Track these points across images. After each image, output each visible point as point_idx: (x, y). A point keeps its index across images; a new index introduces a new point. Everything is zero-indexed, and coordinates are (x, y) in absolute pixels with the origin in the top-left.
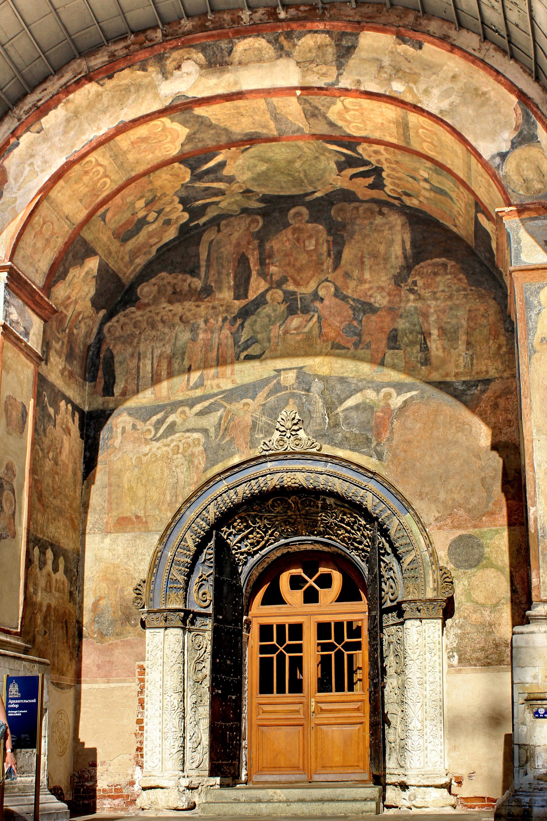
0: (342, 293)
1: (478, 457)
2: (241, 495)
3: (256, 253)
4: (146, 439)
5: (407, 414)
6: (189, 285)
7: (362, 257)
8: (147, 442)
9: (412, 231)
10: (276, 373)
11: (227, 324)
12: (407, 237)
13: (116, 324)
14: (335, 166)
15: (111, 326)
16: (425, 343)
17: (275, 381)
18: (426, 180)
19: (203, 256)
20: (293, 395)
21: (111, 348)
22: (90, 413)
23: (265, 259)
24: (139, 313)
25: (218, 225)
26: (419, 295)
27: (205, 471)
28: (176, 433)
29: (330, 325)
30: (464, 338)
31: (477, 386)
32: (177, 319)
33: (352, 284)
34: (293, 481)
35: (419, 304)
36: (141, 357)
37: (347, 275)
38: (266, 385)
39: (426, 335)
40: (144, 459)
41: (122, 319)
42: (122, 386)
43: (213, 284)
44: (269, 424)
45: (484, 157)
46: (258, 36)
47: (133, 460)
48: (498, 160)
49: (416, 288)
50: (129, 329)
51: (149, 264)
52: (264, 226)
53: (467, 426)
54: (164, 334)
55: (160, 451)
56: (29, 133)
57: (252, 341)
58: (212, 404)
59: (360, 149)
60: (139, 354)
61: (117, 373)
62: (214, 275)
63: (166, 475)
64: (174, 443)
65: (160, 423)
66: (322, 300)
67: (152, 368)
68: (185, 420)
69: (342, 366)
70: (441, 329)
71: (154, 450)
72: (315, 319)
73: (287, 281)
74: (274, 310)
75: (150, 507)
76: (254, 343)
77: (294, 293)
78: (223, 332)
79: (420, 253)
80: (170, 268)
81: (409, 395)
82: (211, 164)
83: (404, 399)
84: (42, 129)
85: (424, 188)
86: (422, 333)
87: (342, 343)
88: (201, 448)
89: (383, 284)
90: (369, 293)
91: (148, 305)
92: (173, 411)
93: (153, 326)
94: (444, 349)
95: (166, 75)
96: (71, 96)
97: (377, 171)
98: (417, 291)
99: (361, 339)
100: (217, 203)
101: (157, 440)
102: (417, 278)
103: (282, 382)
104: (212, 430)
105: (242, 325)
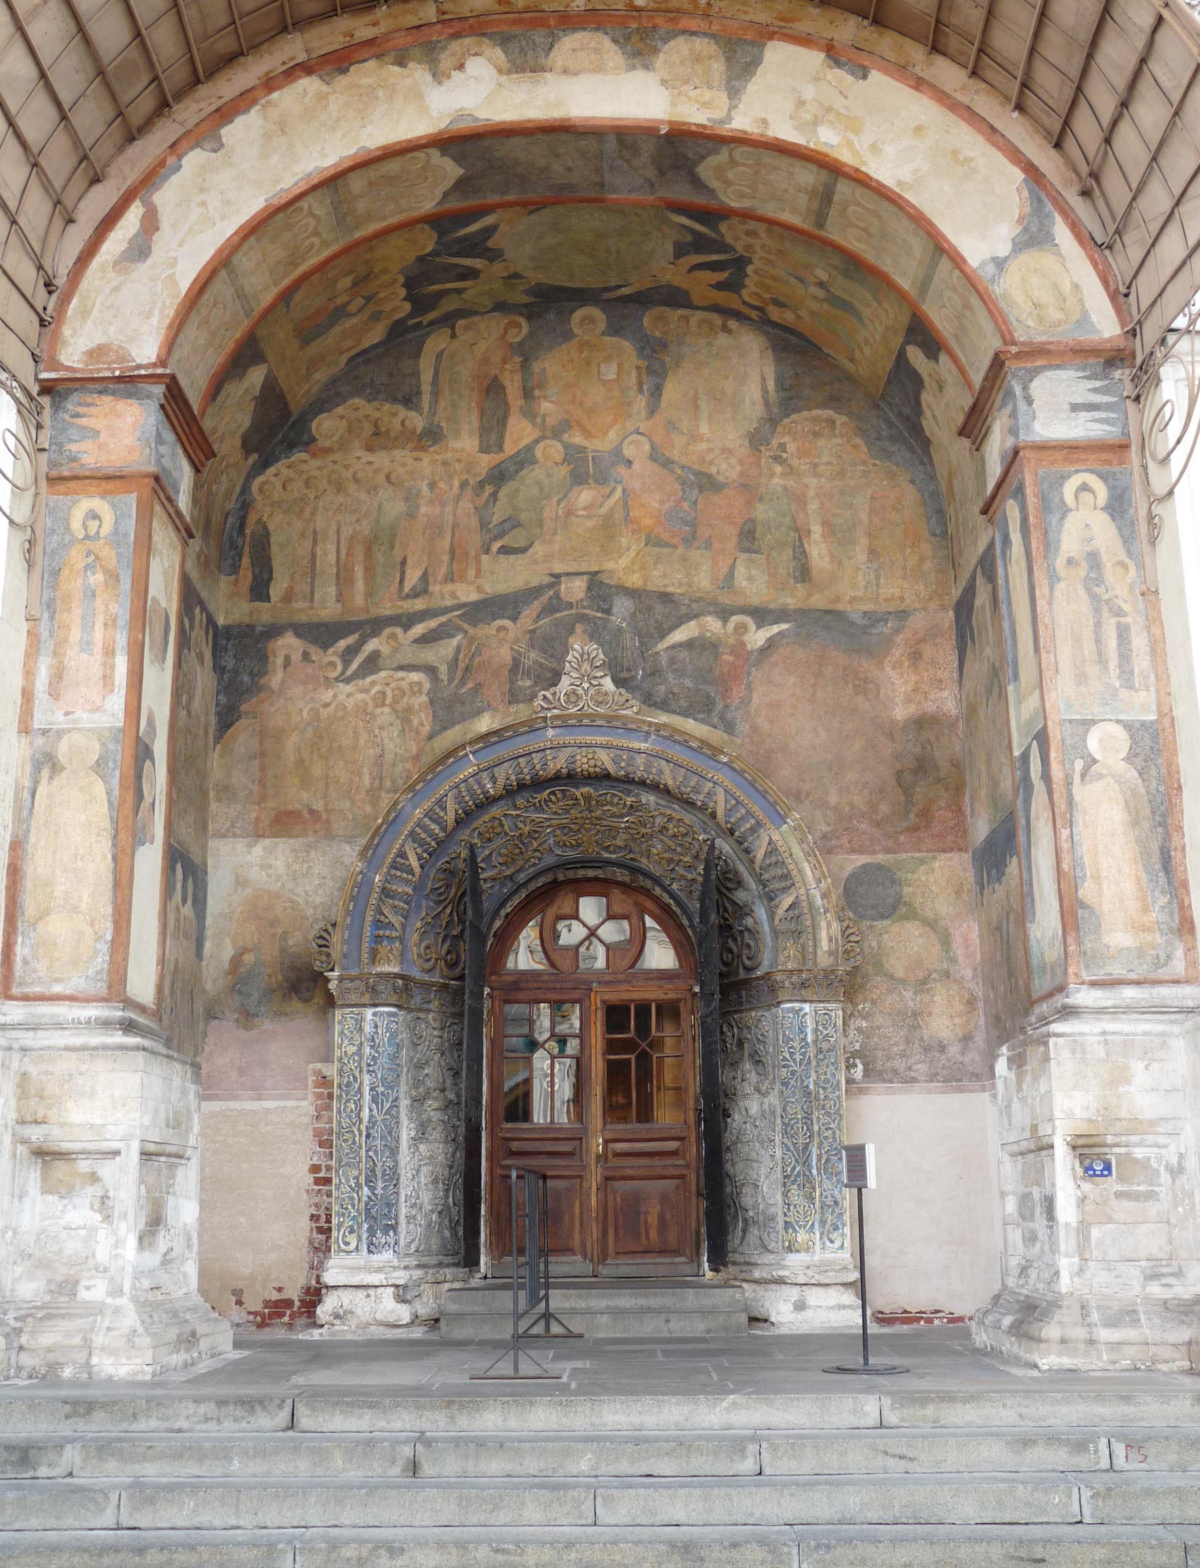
0: (663, 455)
1: (891, 736)
2: (501, 782)
3: (518, 377)
4: (327, 678)
5: (773, 659)
6: (403, 423)
7: (696, 398)
8: (328, 683)
9: (778, 361)
10: (553, 580)
11: (469, 492)
12: (770, 371)
13: (273, 479)
14: (671, 249)
15: (266, 482)
16: (802, 546)
17: (551, 593)
18: (821, 285)
19: (427, 376)
20: (582, 618)
21: (264, 519)
22: (228, 629)
23: (532, 390)
24: (314, 463)
25: (453, 328)
26: (790, 466)
27: (430, 737)
28: (380, 670)
29: (643, 506)
30: (864, 541)
31: (886, 621)
32: (381, 478)
33: (679, 441)
34: (592, 763)
35: (791, 483)
36: (319, 537)
37: (671, 426)
38: (536, 598)
39: (801, 533)
40: (324, 713)
41: (285, 472)
42: (285, 585)
43: (443, 424)
44: (541, 665)
45: (970, 261)
46: (597, 29)
47: (305, 714)
48: (991, 269)
49: (784, 455)
50: (297, 488)
51: (335, 381)
52: (531, 334)
53: (870, 686)
54: (359, 501)
55: (351, 700)
56: (198, 150)
57: (512, 523)
58: (442, 625)
59: (723, 227)
60: (315, 533)
61: (275, 563)
62: (445, 408)
63: (362, 742)
64: (377, 688)
65: (352, 652)
66: (629, 463)
67: (338, 557)
68: (395, 650)
69: (665, 576)
70: (825, 523)
71: (341, 697)
72: (618, 493)
73: (571, 427)
74: (549, 475)
75: (334, 795)
76: (514, 527)
77: (582, 449)
78: (460, 505)
79: (791, 399)
80: (368, 391)
81: (776, 629)
82: (475, 227)
83: (769, 635)
84: (222, 145)
85: (814, 297)
86: (797, 530)
87: (665, 536)
88: (424, 699)
89: (729, 445)
90: (708, 458)
91: (329, 450)
92: (376, 633)
93: (339, 488)
94: (832, 557)
95: (439, 77)
97: (740, 263)
98: (786, 460)
99: (695, 532)
100: (459, 291)
101: (347, 681)
102: (787, 439)
103: (562, 595)
104: (443, 669)
105: (494, 495)
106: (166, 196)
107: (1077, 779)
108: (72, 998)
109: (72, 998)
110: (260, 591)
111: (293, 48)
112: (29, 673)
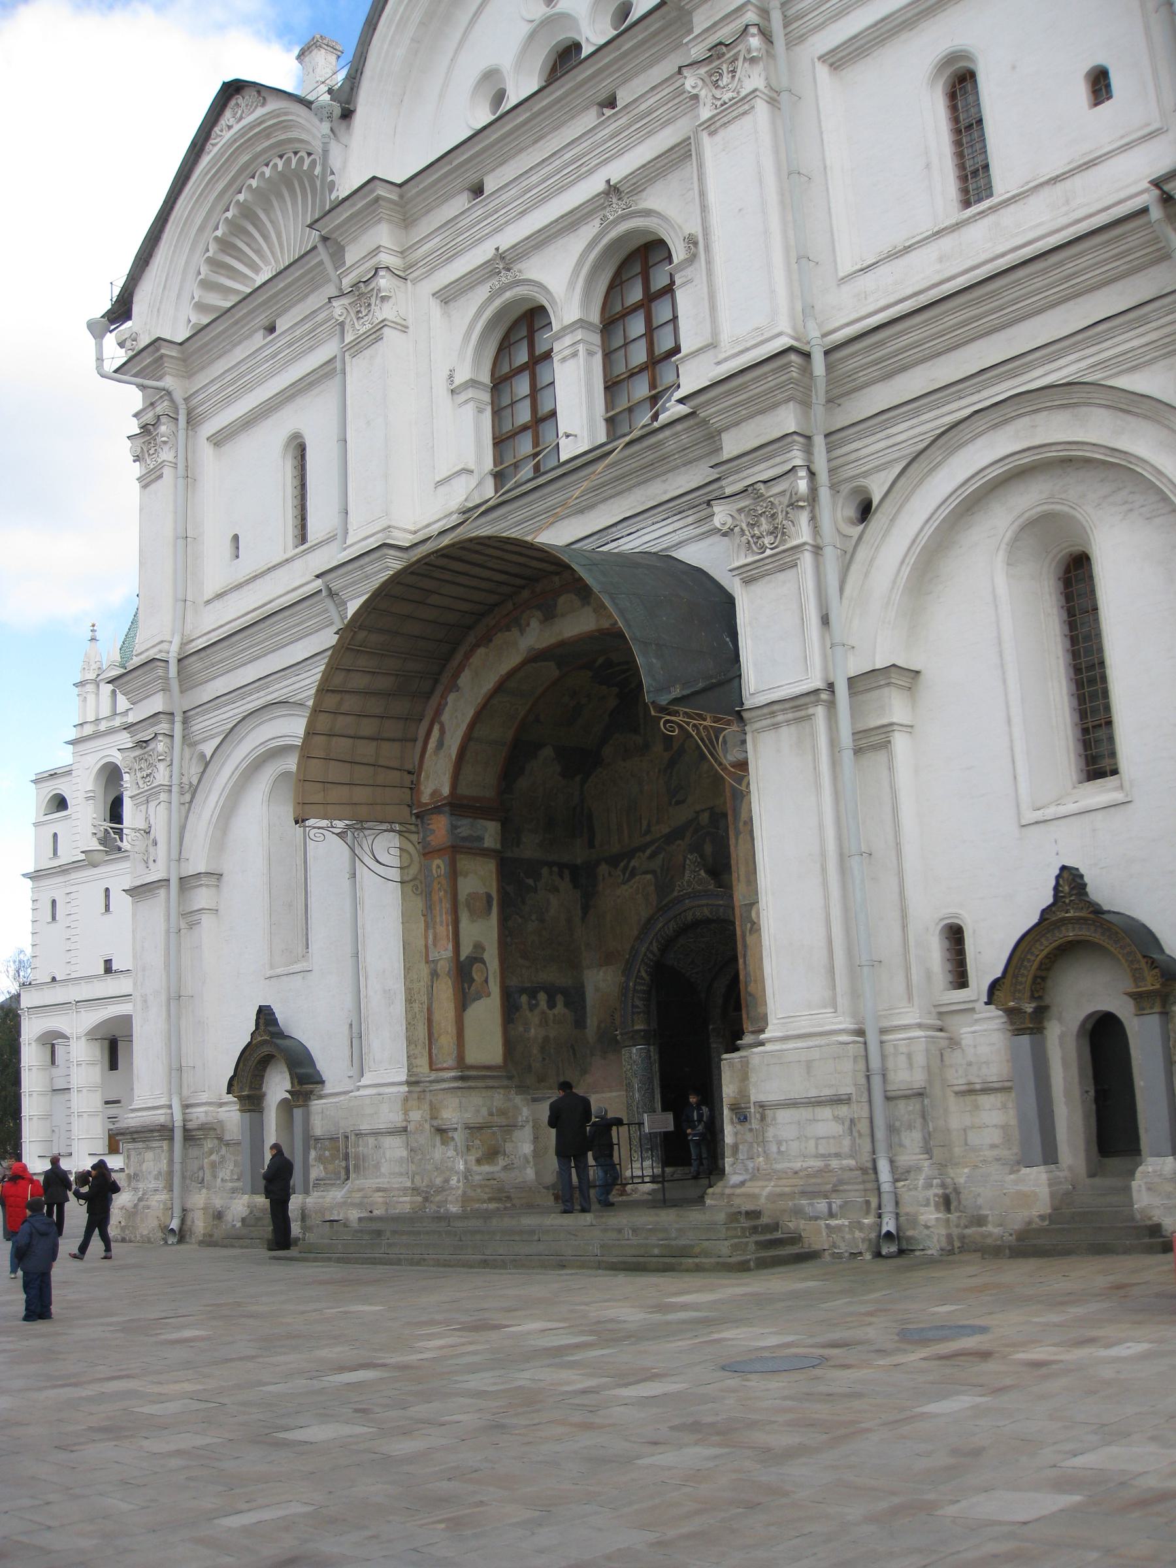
88: (652, 888)
96: (471, 660)
101: (624, 883)
106: (445, 717)
107: (748, 934)
108: (448, 1069)
109: (448, 1069)
110: (591, 845)
111: (471, 639)
112: (426, 938)
